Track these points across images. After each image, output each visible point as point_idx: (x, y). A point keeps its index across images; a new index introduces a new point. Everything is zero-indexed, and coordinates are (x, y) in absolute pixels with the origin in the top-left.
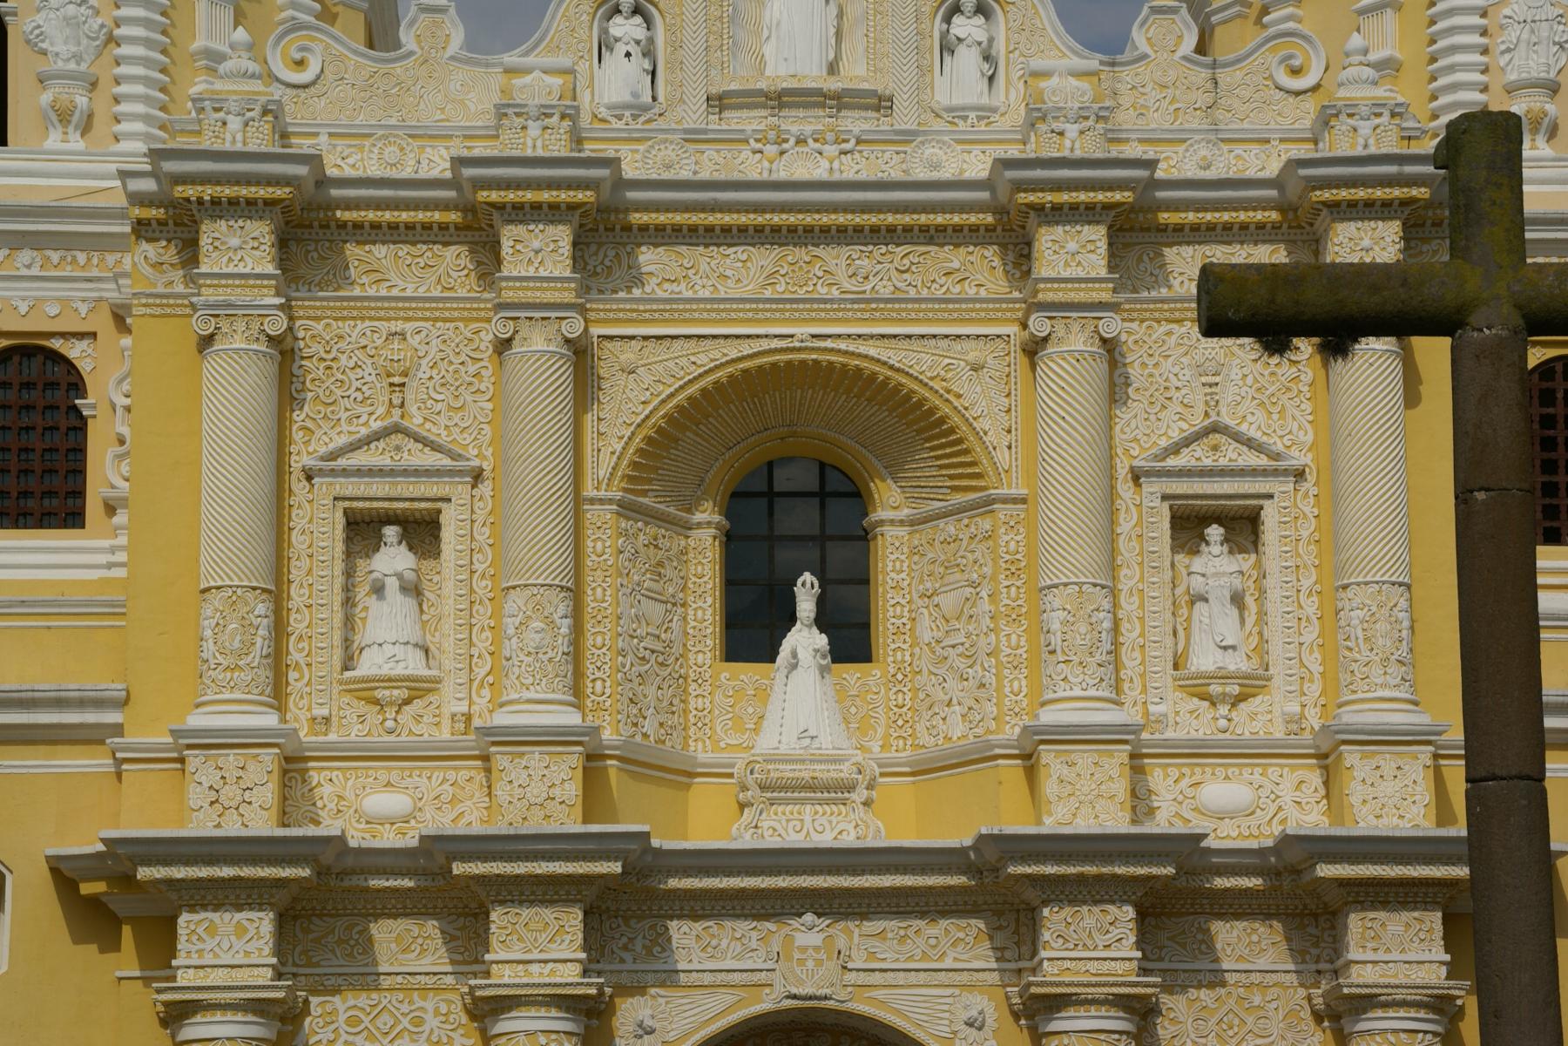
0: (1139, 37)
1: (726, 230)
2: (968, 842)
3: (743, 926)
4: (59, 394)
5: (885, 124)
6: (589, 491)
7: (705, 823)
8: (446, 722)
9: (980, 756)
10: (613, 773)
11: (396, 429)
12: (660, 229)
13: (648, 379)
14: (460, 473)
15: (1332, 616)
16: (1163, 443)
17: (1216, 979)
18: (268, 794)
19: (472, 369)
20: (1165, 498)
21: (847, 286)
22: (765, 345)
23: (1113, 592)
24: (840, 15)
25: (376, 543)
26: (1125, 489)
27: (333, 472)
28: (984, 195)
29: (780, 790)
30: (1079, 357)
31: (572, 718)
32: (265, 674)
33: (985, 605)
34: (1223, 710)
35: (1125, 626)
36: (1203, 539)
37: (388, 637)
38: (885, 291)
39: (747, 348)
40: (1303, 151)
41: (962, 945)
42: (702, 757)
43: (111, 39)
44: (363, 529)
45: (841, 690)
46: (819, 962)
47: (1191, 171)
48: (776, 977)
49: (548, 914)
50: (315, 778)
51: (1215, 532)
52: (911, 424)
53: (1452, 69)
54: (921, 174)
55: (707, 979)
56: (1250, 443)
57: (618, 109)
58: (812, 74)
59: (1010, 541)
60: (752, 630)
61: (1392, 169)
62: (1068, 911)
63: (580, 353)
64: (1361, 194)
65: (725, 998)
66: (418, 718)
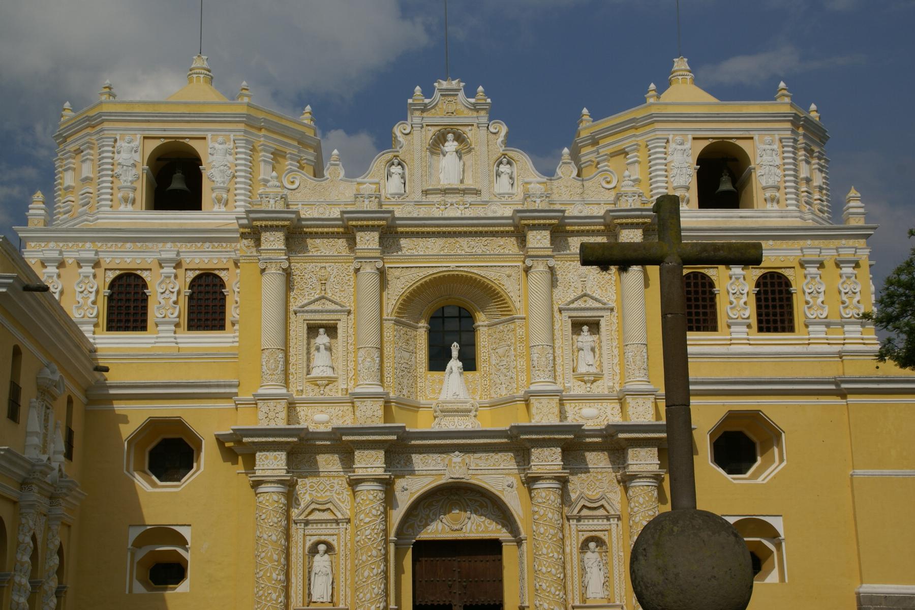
0: (559, 171)
1: (428, 233)
2: (508, 428)
3: (435, 456)
4: (218, 288)
5: (479, 199)
6: (385, 317)
7: (423, 423)
8: (340, 391)
9: (511, 401)
10: (393, 407)
11: (323, 298)
12: (407, 233)
13: (404, 281)
14: (344, 311)
15: (623, 354)
16: (569, 300)
17: (587, 471)
18: (283, 415)
19: (347, 278)
20: (570, 317)
21: (467, 250)
22: (441, 269)
23: (553, 348)
24: (464, 165)
25: (317, 334)
26: (557, 314)
27: (303, 312)
28: (511, 221)
29: (448, 412)
30: (542, 272)
31: (380, 390)
32: (282, 376)
33: (513, 352)
34: (589, 385)
35: (557, 359)
36: (582, 330)
37: (321, 364)
38: (480, 252)
39: (435, 270)
40: (611, 207)
41: (506, 461)
42: (422, 402)
43: (234, 177)
44: (313, 330)
45: (466, 380)
46: (460, 467)
47: (576, 214)
48: (446, 472)
49: (373, 452)
50: (298, 409)
51: (585, 328)
52: (488, 294)
53: (656, 182)
54: (491, 215)
55: (425, 473)
56: (596, 300)
57: (393, 195)
58: (455, 184)
59: (520, 332)
60: (438, 361)
61: (639, 213)
62: (540, 450)
63: (382, 273)
64: (629, 221)
65: (430, 479)
66: (331, 390)
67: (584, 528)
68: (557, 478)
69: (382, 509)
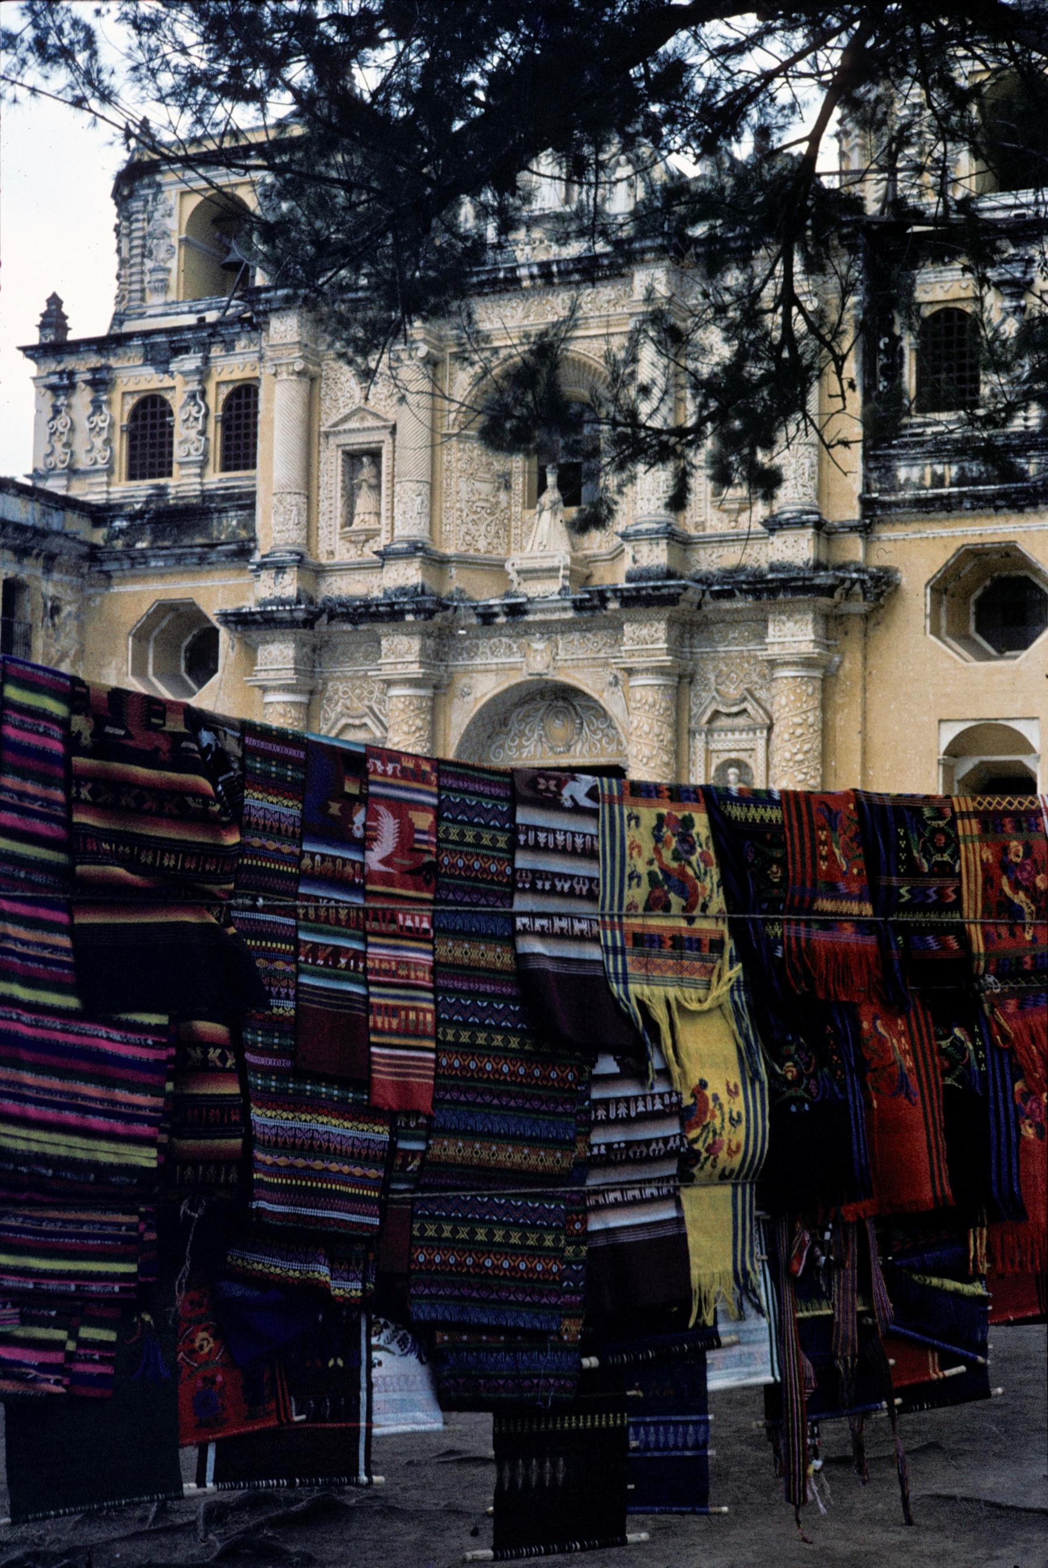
27: (337, 434)
67: (720, 747)
68: (660, 671)
69: (419, 723)
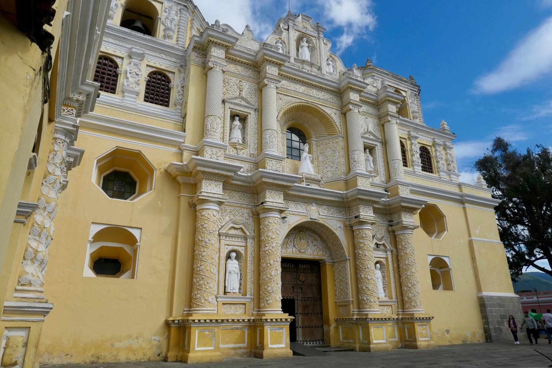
55: (296, 213)
65: (298, 218)
66: (244, 153)
